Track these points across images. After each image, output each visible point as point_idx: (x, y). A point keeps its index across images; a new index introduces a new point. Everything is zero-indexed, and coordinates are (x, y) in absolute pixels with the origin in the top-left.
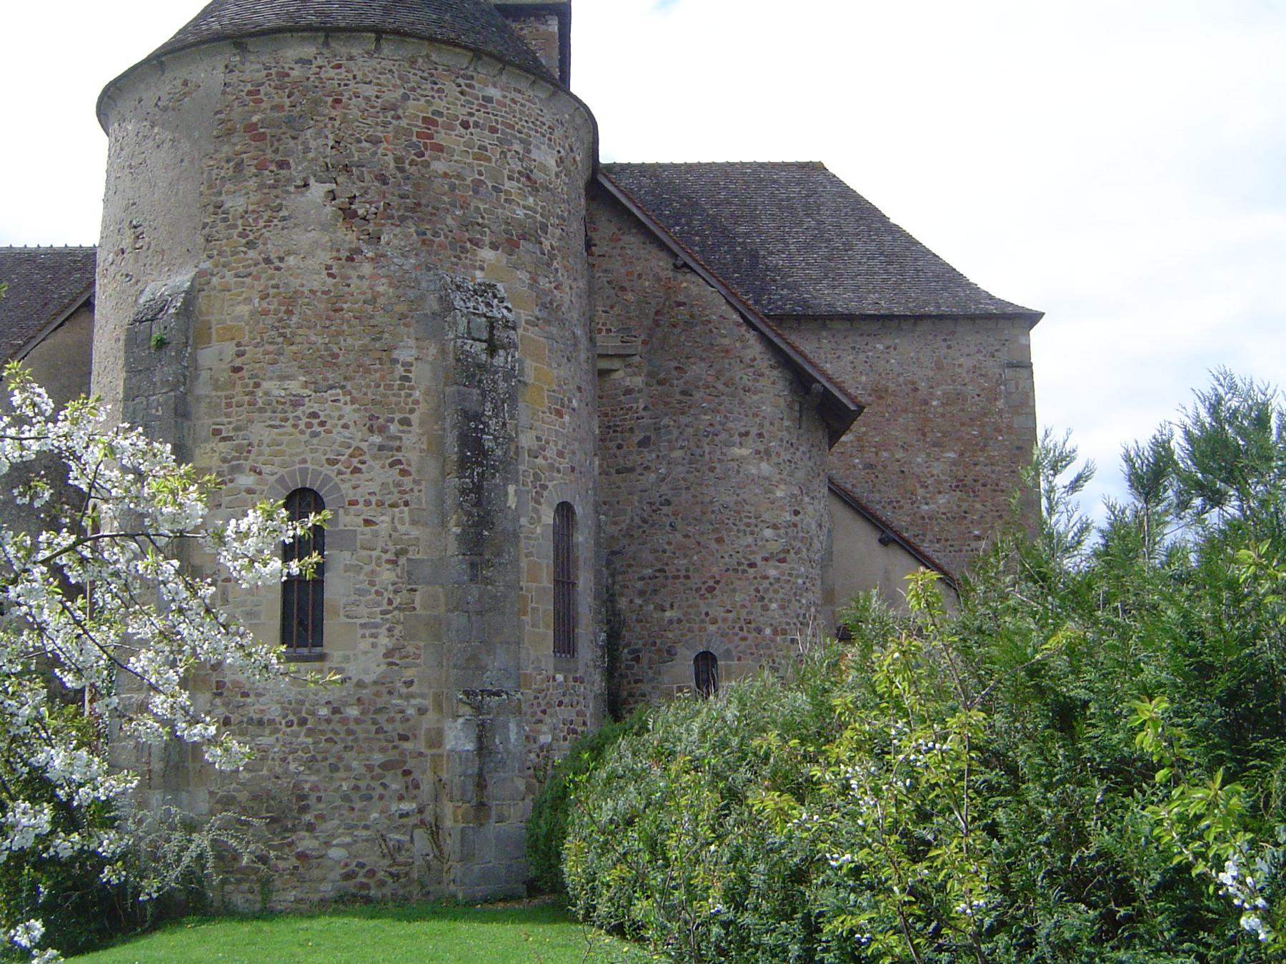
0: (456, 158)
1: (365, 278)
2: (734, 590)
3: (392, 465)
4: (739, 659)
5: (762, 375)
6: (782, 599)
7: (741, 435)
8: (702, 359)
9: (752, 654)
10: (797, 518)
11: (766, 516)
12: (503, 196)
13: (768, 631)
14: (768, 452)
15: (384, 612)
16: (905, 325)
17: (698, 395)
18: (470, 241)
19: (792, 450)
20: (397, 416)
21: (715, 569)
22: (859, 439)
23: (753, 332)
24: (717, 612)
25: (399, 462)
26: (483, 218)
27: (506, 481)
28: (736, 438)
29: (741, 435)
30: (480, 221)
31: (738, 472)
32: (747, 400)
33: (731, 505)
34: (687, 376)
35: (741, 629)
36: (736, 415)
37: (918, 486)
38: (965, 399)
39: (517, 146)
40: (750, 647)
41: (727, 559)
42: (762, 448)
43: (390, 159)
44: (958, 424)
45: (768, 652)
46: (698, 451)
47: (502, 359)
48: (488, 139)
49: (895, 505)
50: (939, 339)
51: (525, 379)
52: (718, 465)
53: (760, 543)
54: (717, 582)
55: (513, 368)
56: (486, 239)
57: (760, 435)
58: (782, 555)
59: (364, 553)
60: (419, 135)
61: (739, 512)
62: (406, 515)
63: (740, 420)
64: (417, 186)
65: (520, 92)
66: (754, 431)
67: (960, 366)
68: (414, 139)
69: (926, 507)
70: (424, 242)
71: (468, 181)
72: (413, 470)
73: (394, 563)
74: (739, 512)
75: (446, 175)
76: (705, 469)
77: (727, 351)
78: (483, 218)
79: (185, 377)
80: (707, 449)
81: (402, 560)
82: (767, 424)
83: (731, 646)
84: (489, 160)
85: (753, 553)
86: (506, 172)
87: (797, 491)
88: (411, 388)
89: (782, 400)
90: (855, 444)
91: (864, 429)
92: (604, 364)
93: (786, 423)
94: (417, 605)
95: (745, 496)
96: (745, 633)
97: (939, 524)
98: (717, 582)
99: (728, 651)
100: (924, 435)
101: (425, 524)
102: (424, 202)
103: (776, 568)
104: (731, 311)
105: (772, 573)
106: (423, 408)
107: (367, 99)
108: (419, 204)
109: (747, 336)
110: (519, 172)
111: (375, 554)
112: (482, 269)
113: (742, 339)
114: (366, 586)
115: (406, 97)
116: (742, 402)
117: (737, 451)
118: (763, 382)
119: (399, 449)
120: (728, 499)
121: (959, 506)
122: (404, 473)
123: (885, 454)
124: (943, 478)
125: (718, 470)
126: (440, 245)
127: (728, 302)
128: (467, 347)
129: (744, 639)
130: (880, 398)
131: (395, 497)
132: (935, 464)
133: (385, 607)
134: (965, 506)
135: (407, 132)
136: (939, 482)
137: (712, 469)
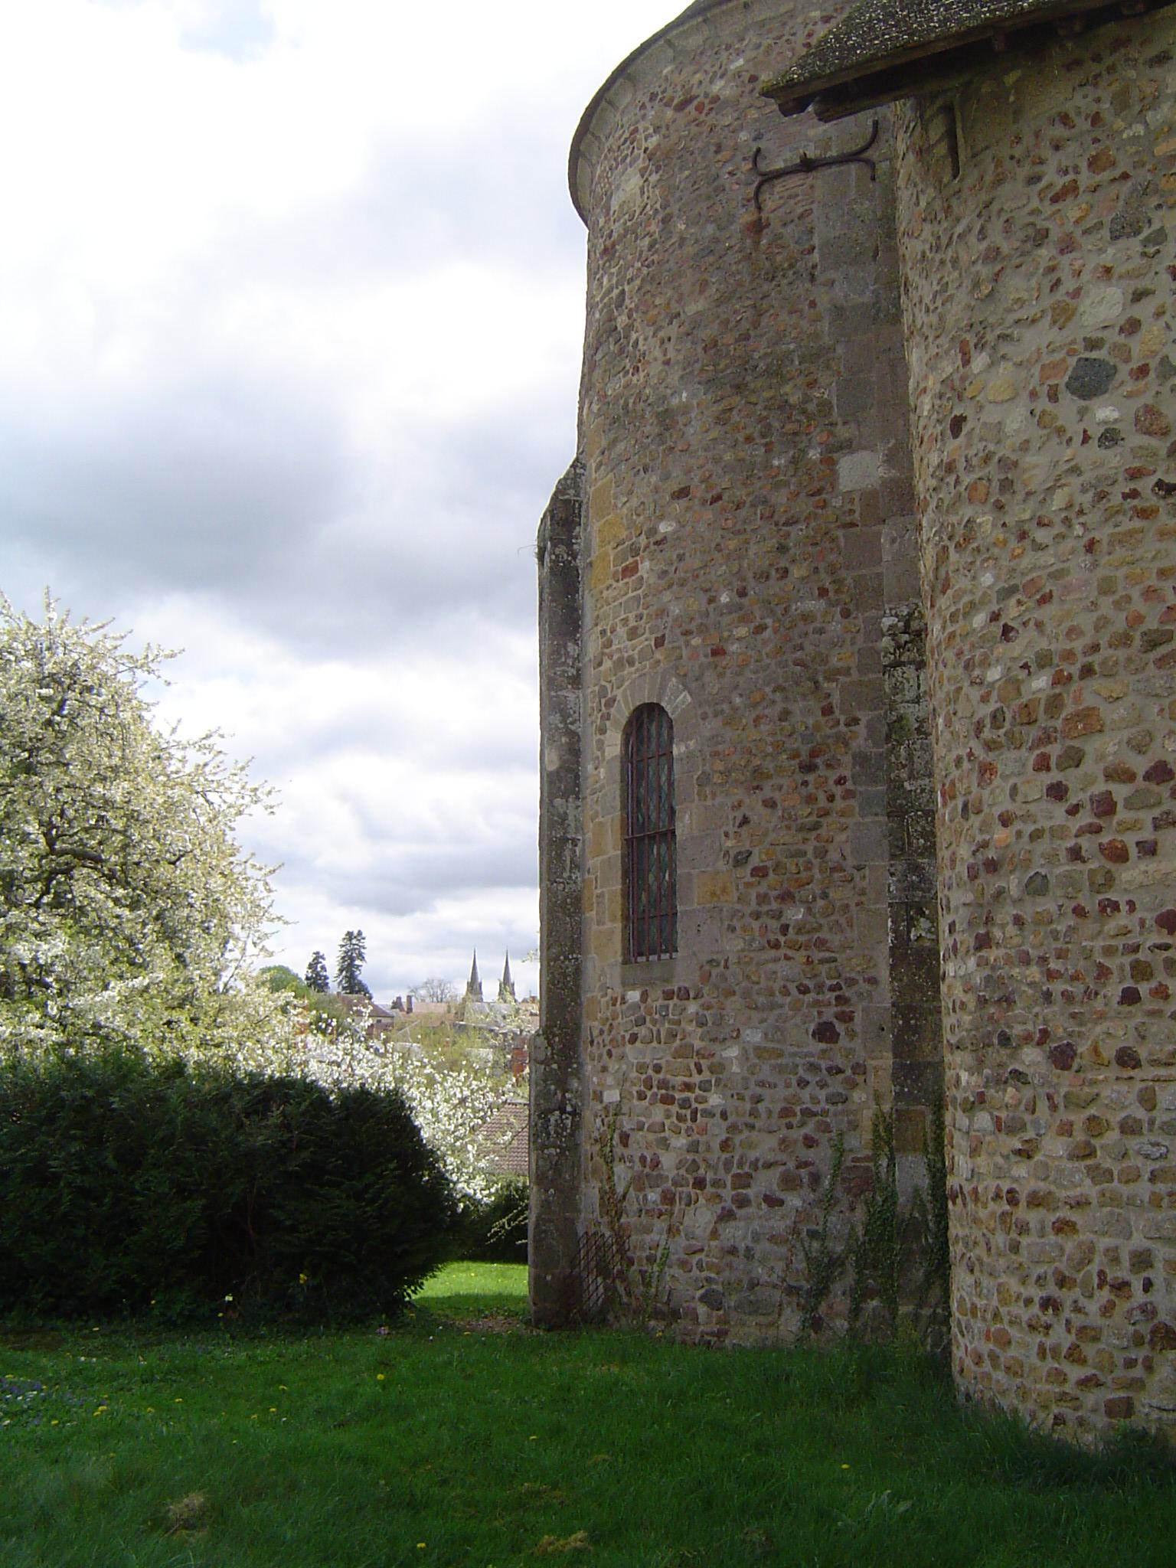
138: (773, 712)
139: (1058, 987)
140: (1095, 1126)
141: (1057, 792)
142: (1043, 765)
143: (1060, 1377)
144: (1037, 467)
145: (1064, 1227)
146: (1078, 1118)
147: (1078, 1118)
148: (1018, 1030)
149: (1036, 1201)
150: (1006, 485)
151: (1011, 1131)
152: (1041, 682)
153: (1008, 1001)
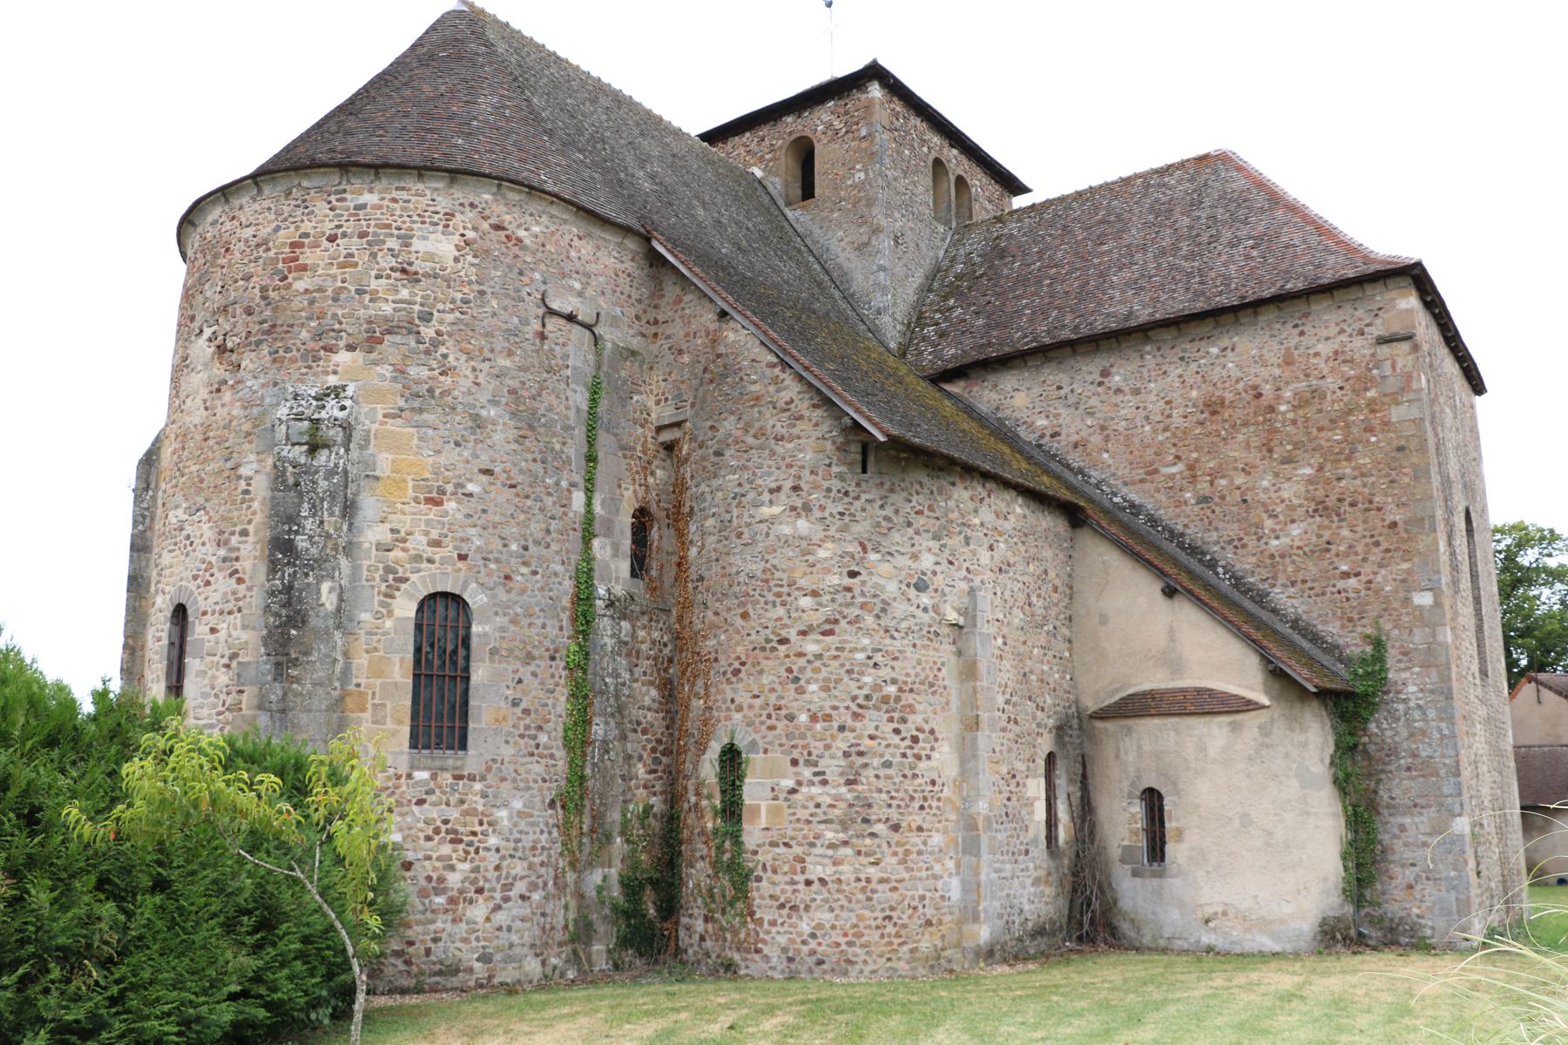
0: (320, 272)
1: (229, 407)
2: (761, 672)
3: (231, 575)
4: (766, 751)
5: (801, 418)
6: (825, 680)
7: (771, 491)
8: (733, 413)
9: (781, 745)
10: (856, 580)
11: (801, 582)
12: (367, 297)
13: (803, 718)
14: (807, 508)
15: (219, 714)
16: (1245, 317)
17: (728, 453)
18: (324, 348)
19: (846, 500)
20: (238, 528)
21: (739, 649)
22: (1191, 468)
23: (788, 371)
24: (743, 698)
25: (236, 571)
26: (340, 323)
27: (320, 580)
28: (766, 497)
29: (771, 491)
30: (337, 326)
31: (768, 534)
32: (780, 450)
33: (759, 573)
34: (720, 435)
35: (769, 716)
36: (765, 469)
37: (1265, 516)
38: (1323, 397)
39: (392, 243)
40: (778, 737)
41: (754, 637)
42: (799, 503)
43: (257, 291)
44: (1315, 431)
45: (801, 742)
46: (728, 517)
47: (324, 458)
48: (355, 244)
49: (1238, 544)
50: (1289, 325)
51: (377, 473)
52: (746, 530)
53: (794, 615)
54: (743, 664)
55: (336, 465)
56: (342, 343)
57: (796, 488)
58: (827, 627)
59: (209, 659)
60: (284, 261)
61: (767, 581)
62: (238, 621)
63: (770, 474)
64: (275, 310)
65: (403, 189)
66: (788, 484)
67: (1317, 354)
68: (280, 265)
69: (1276, 542)
70: (274, 361)
71: (330, 292)
72: (246, 577)
73: (228, 666)
74: (767, 581)
75: (307, 291)
76: (733, 535)
77: (757, 399)
78: (340, 323)
79: (144, 517)
80: (735, 512)
81: (234, 664)
82: (806, 472)
83: (757, 737)
84: (356, 264)
85: (786, 626)
86: (373, 273)
87: (853, 548)
88: (252, 500)
89: (828, 445)
90: (1187, 473)
91: (1195, 455)
92: (666, 436)
93: (835, 469)
94: (243, 706)
95: (776, 562)
96: (773, 722)
97: (1293, 562)
98: (743, 664)
99: (753, 743)
100: (1270, 451)
101: (254, 628)
102: (279, 322)
103: (817, 642)
104: (764, 350)
105: (811, 648)
106: (258, 518)
107: (247, 241)
108: (274, 326)
109: (782, 376)
110: (392, 269)
111: (216, 659)
112: (335, 372)
113: (776, 381)
114: (208, 689)
115: (278, 229)
116: (772, 453)
117: (766, 511)
118: (800, 425)
119: (237, 559)
120: (754, 567)
121: (1319, 536)
122: (240, 581)
123: (1223, 482)
124: (1296, 502)
125: (746, 536)
126: (293, 360)
127: (762, 343)
128: (284, 453)
129: (772, 728)
130: (1214, 413)
131: (230, 606)
132: (1286, 485)
133: (220, 708)
134: (1327, 534)
135: (275, 261)
136: (1292, 508)
137: (739, 535)
138: (539, 622)
139: (894, 803)
140: (907, 853)
141: (897, 731)
142: (891, 720)
143: (891, 943)
144: (900, 608)
145: (895, 889)
146: (900, 850)
147: (900, 850)
148: (874, 817)
149: (882, 881)
150: (884, 610)
151: (867, 855)
152: (892, 689)
153: (870, 806)
